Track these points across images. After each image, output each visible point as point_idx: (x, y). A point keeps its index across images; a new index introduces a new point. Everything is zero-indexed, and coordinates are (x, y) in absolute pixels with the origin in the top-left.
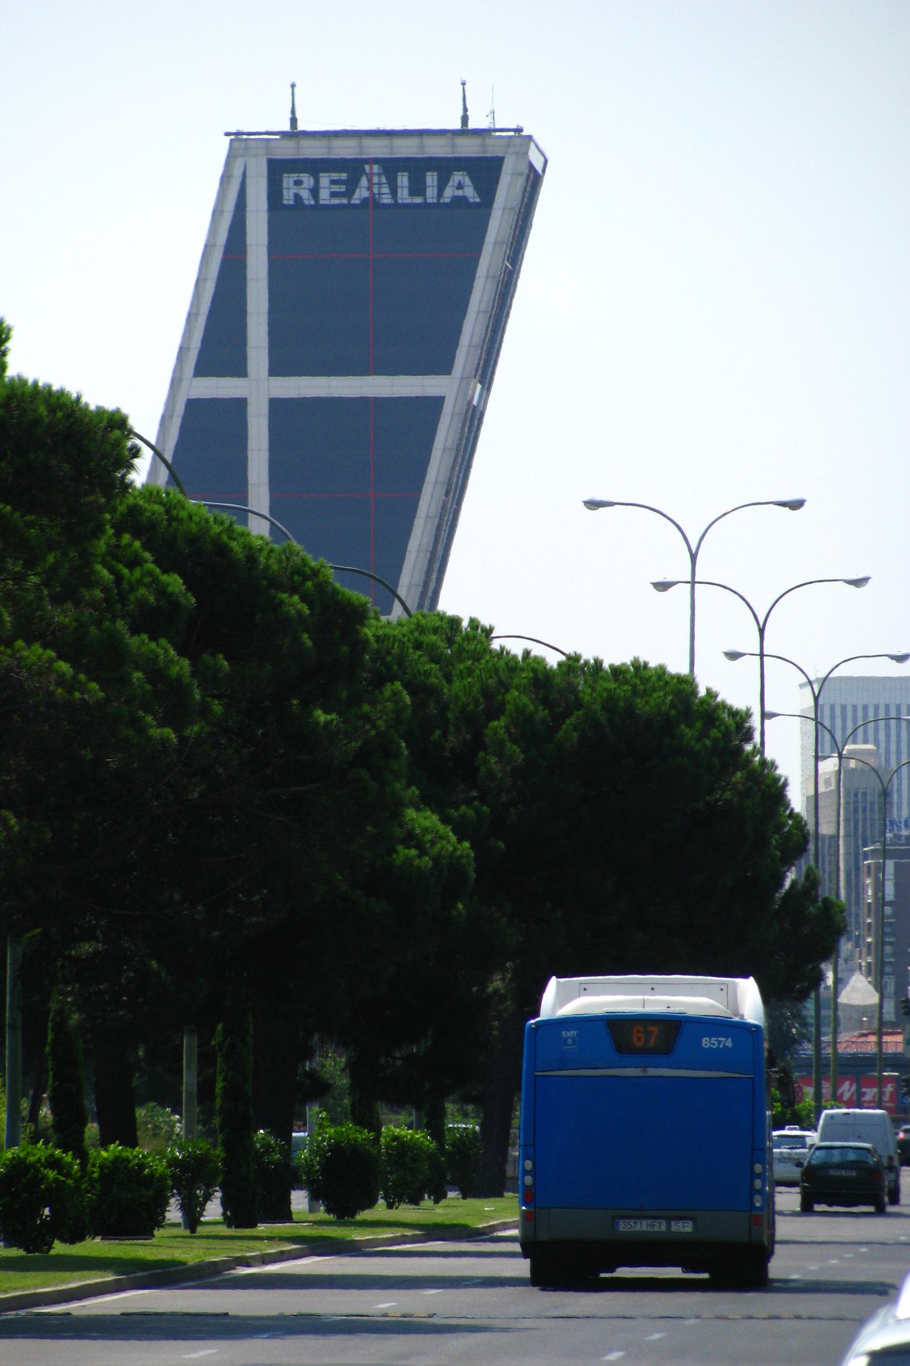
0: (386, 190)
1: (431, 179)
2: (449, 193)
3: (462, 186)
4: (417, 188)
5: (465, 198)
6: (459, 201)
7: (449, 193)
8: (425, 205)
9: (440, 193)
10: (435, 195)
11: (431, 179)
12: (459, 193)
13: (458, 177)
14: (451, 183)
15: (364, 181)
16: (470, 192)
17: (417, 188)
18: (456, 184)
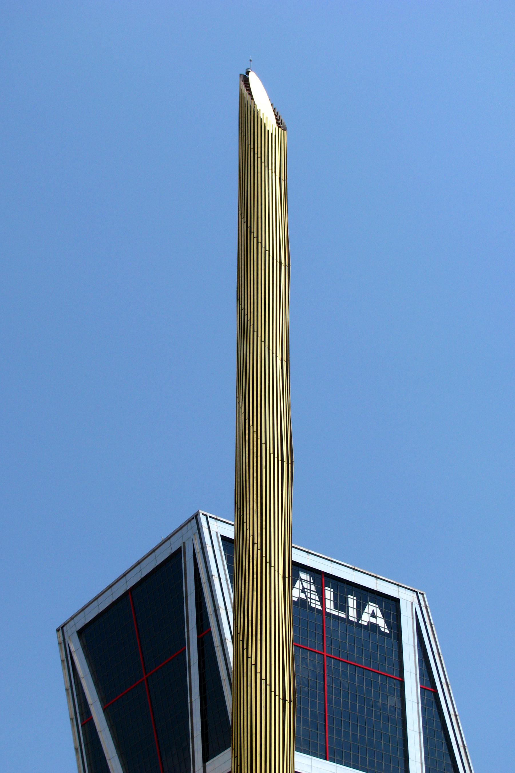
0: (315, 596)
1: (352, 602)
2: (366, 618)
3: (373, 615)
4: (341, 604)
5: (379, 627)
6: (373, 627)
7: (366, 618)
8: (347, 620)
9: (359, 615)
10: (356, 616)
11: (352, 602)
12: (373, 620)
13: (371, 607)
14: (366, 610)
15: (298, 584)
16: (381, 622)
17: (341, 604)
18: (371, 612)
